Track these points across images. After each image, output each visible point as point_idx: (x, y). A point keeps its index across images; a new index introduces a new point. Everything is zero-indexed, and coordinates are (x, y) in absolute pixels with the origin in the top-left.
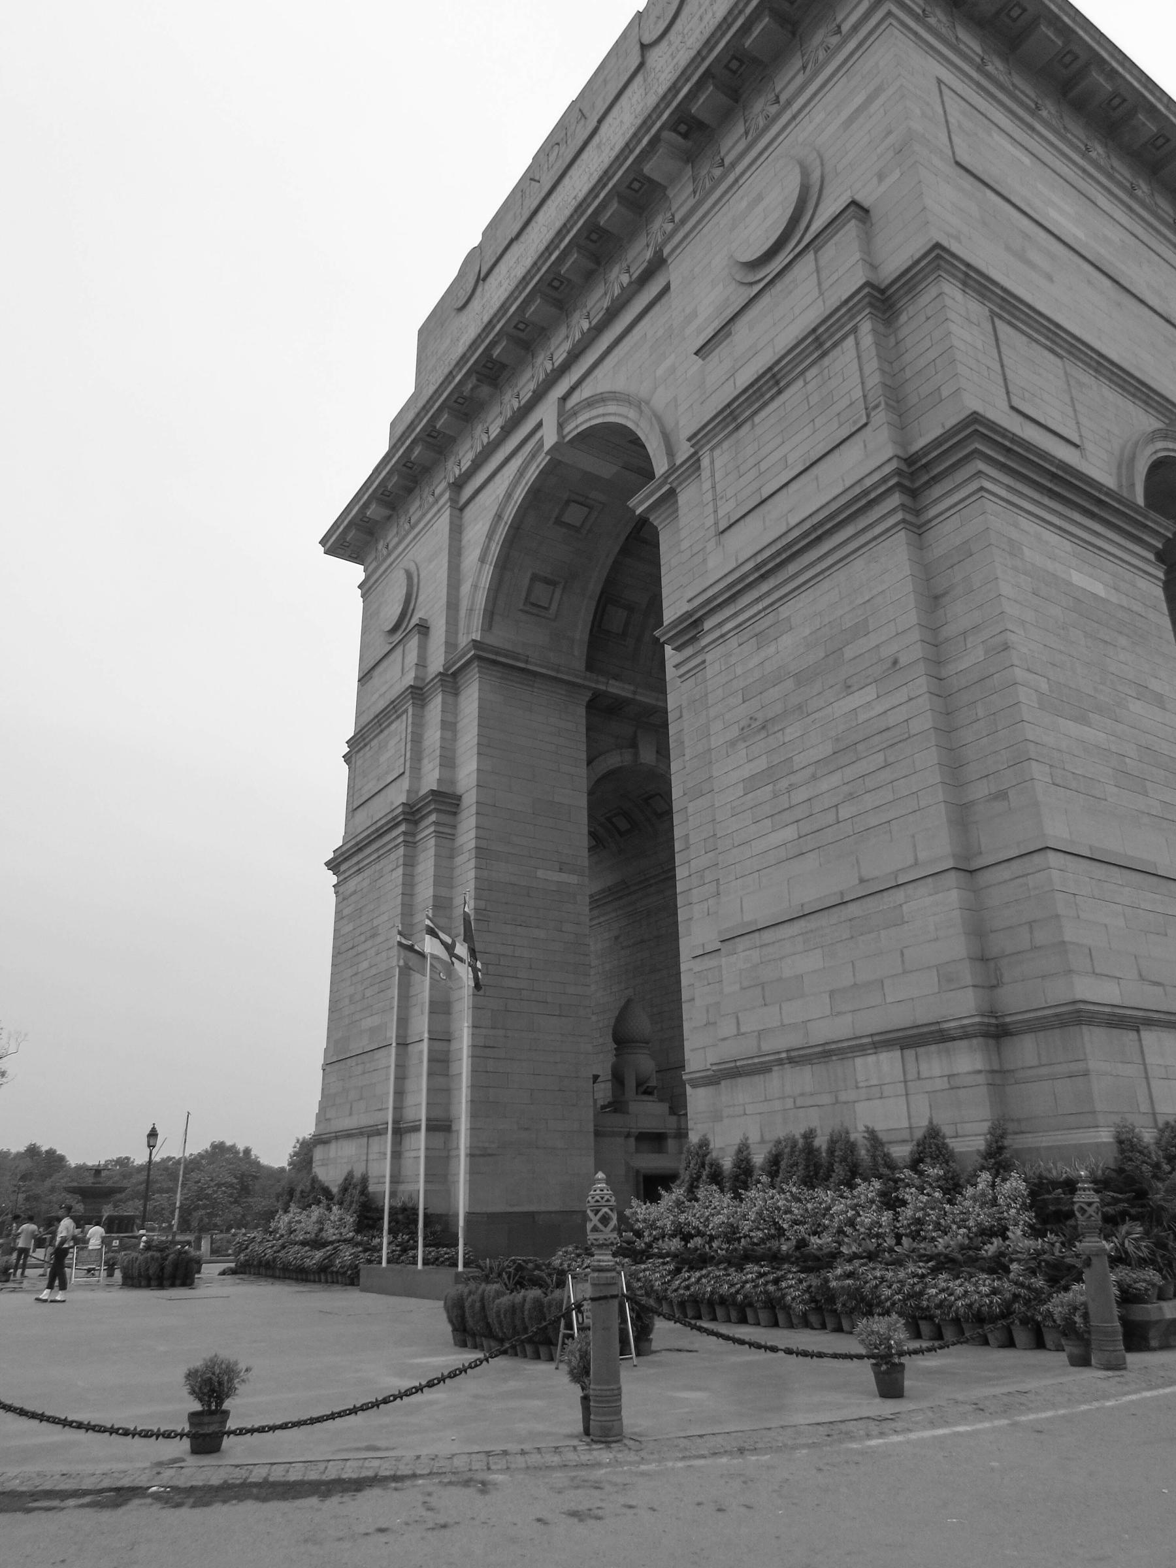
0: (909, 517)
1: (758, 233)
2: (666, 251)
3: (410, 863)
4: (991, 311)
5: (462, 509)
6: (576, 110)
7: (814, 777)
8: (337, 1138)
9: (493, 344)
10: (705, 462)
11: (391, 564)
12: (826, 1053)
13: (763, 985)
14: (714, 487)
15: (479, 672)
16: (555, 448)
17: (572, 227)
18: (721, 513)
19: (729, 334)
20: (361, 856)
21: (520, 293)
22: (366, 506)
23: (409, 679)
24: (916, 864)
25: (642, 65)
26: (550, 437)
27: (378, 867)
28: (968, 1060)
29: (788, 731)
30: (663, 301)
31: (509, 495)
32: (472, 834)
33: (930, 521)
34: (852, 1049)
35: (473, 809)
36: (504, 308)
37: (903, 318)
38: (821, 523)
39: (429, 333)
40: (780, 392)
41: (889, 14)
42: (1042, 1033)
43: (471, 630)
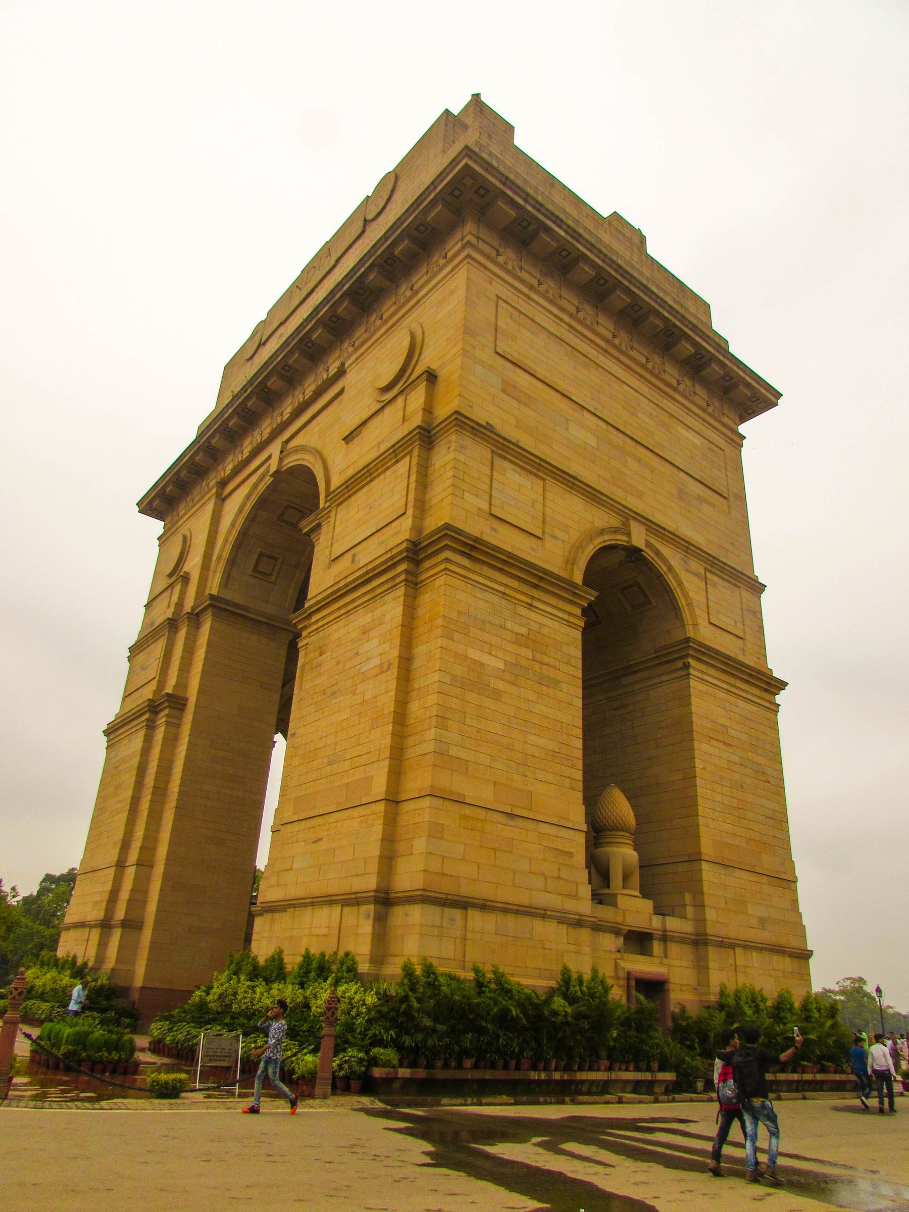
0: (410, 578)
1: (388, 371)
2: (346, 365)
4: (493, 452)
5: (224, 500)
6: (327, 248)
15: (213, 616)
16: (277, 472)
19: (360, 433)
23: (169, 614)
26: (273, 466)
31: (248, 497)
33: (421, 582)
39: (229, 369)
41: (469, 256)
42: (420, 906)
43: (214, 586)
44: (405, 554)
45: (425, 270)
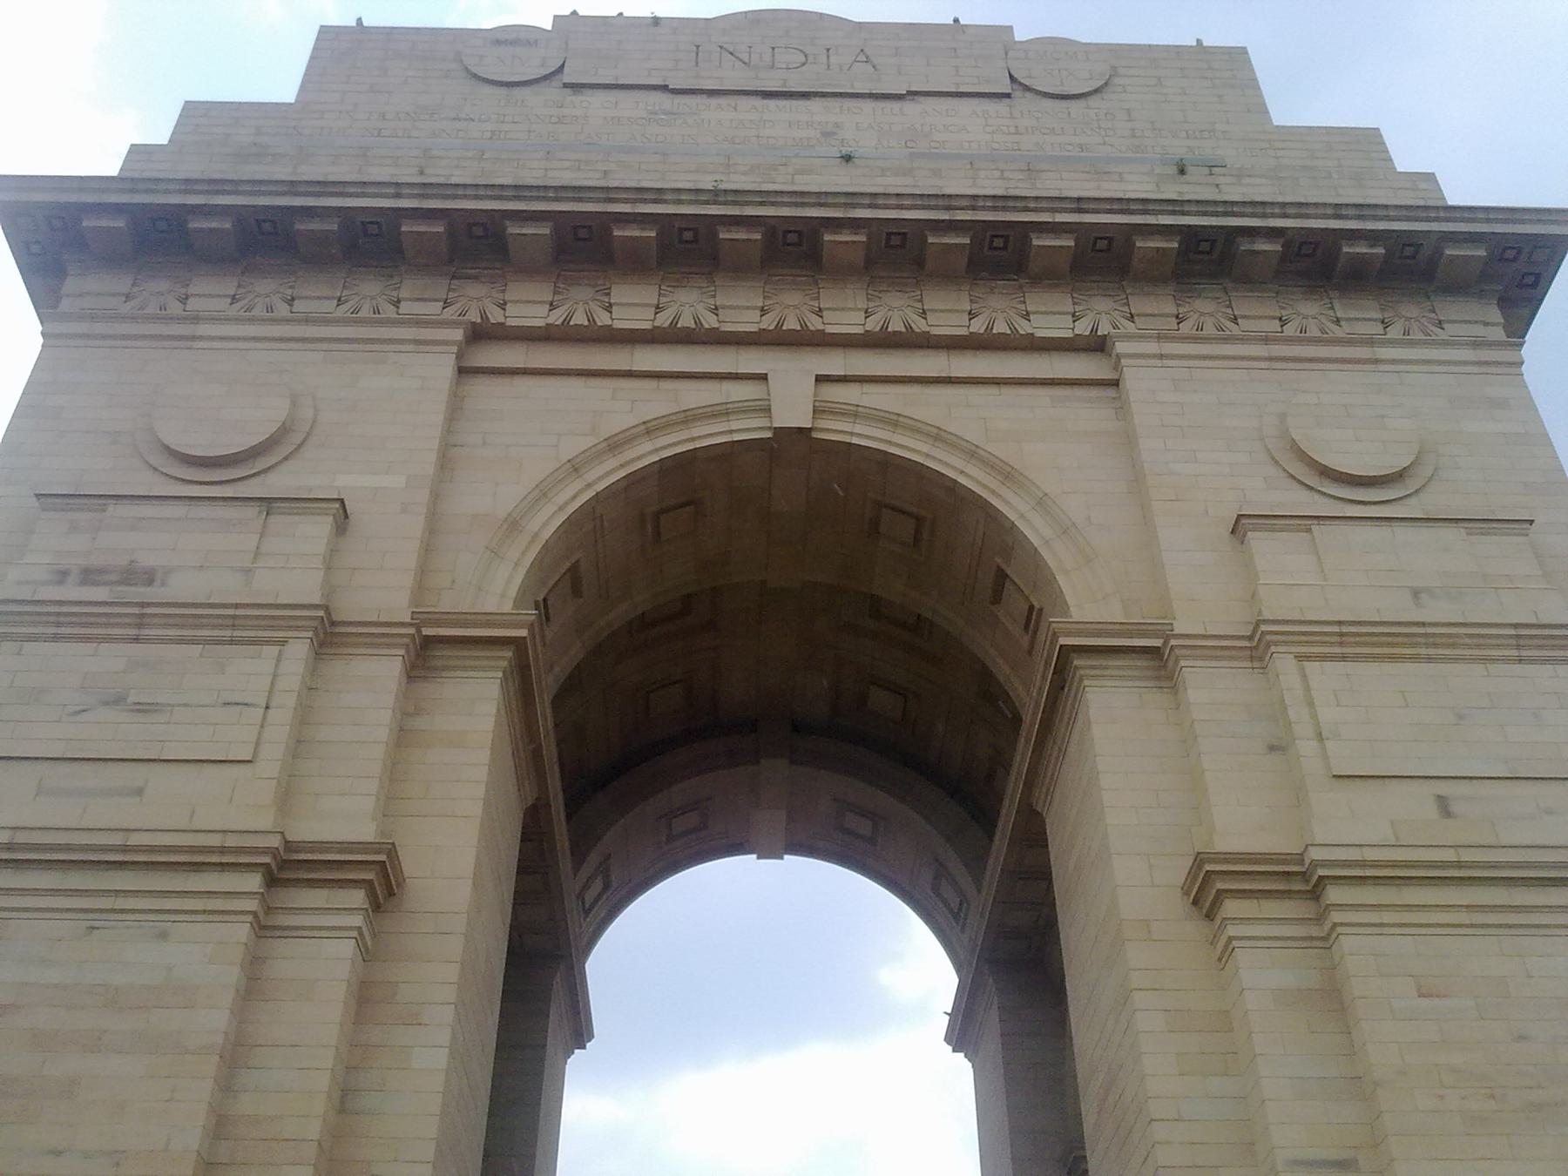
2: (1121, 347)
11: (194, 338)
25: (1008, 96)
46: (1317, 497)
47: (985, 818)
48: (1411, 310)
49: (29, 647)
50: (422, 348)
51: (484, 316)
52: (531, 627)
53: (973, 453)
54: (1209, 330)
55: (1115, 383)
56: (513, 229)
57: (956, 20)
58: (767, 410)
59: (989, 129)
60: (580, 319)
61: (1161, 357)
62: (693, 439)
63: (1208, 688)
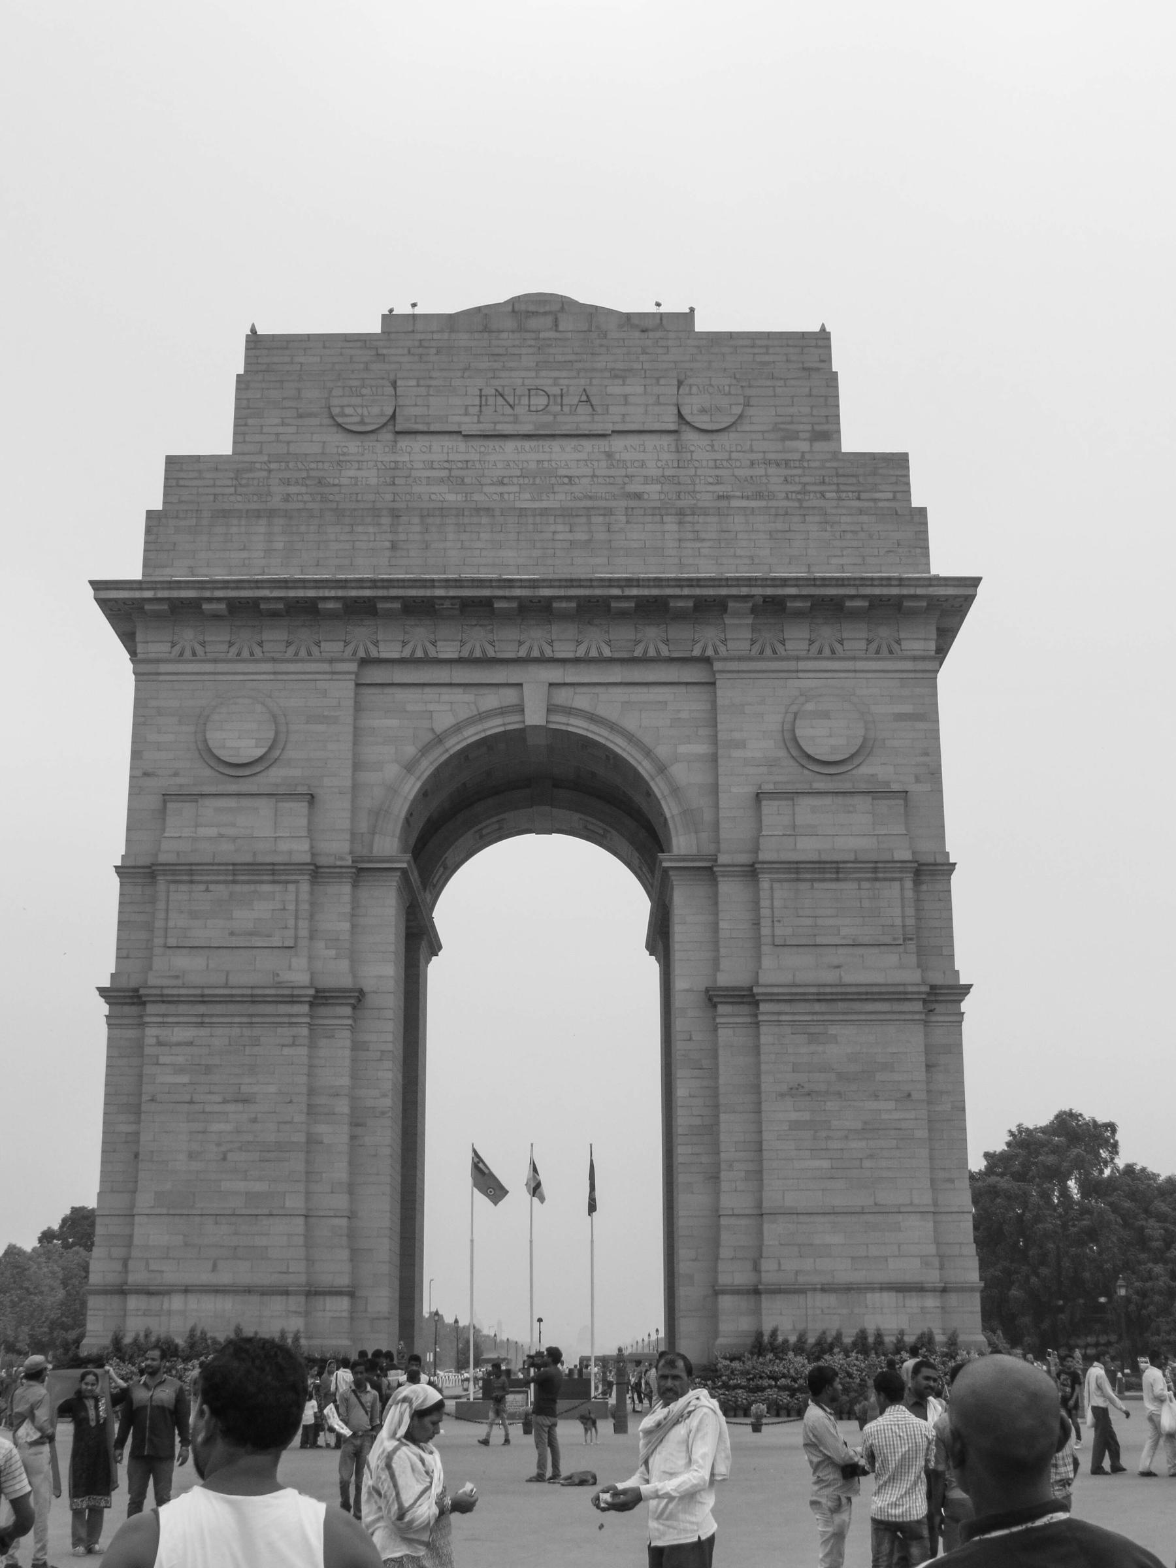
2: (718, 666)
3: (312, 1045)
7: (846, 1137)
8: (186, 1290)
9: (505, 597)
10: (765, 885)
12: (849, 1289)
13: (799, 1245)
14: (772, 908)
17: (643, 586)
18: (778, 932)
20: (202, 1009)
21: (560, 587)
22: (210, 600)
24: (911, 1204)
26: (535, 716)
27: (247, 1032)
28: (931, 1302)
29: (829, 1104)
30: (691, 689)
31: (458, 728)
32: (390, 1037)
34: (866, 1289)
35: (389, 1014)
36: (534, 584)
37: (924, 887)
38: (872, 993)
40: (837, 880)
44: (924, 996)
45: (865, 635)
46: (806, 772)
47: (652, 872)
48: (884, 632)
49: (183, 887)
50: (335, 677)
51: (367, 652)
52: (408, 863)
53: (630, 738)
54: (768, 652)
55: (714, 684)
56: (380, 605)
57: (658, 305)
58: (523, 710)
59: (659, 464)
60: (419, 654)
61: (738, 672)
62: (484, 730)
63: (731, 890)
